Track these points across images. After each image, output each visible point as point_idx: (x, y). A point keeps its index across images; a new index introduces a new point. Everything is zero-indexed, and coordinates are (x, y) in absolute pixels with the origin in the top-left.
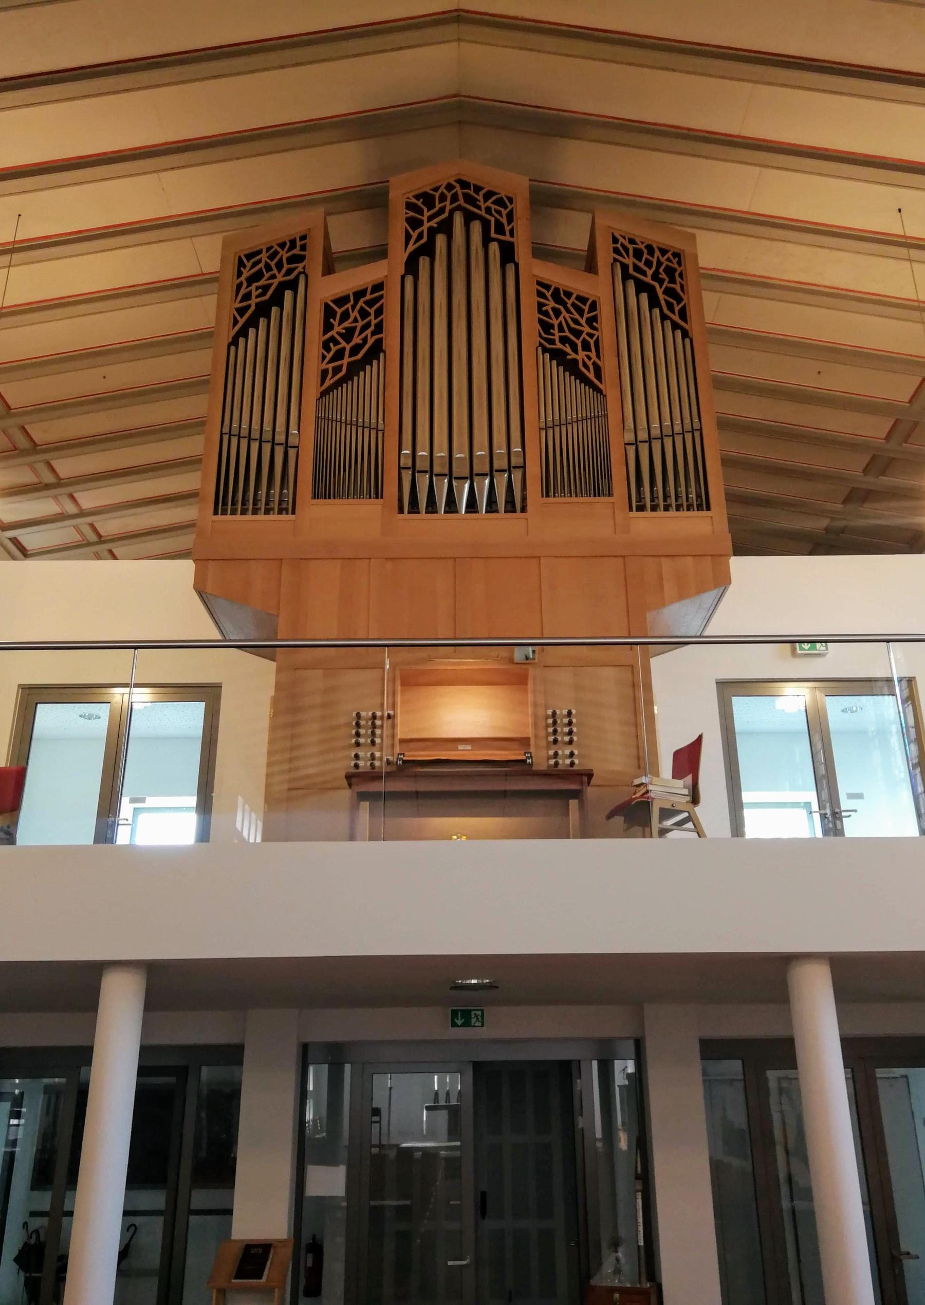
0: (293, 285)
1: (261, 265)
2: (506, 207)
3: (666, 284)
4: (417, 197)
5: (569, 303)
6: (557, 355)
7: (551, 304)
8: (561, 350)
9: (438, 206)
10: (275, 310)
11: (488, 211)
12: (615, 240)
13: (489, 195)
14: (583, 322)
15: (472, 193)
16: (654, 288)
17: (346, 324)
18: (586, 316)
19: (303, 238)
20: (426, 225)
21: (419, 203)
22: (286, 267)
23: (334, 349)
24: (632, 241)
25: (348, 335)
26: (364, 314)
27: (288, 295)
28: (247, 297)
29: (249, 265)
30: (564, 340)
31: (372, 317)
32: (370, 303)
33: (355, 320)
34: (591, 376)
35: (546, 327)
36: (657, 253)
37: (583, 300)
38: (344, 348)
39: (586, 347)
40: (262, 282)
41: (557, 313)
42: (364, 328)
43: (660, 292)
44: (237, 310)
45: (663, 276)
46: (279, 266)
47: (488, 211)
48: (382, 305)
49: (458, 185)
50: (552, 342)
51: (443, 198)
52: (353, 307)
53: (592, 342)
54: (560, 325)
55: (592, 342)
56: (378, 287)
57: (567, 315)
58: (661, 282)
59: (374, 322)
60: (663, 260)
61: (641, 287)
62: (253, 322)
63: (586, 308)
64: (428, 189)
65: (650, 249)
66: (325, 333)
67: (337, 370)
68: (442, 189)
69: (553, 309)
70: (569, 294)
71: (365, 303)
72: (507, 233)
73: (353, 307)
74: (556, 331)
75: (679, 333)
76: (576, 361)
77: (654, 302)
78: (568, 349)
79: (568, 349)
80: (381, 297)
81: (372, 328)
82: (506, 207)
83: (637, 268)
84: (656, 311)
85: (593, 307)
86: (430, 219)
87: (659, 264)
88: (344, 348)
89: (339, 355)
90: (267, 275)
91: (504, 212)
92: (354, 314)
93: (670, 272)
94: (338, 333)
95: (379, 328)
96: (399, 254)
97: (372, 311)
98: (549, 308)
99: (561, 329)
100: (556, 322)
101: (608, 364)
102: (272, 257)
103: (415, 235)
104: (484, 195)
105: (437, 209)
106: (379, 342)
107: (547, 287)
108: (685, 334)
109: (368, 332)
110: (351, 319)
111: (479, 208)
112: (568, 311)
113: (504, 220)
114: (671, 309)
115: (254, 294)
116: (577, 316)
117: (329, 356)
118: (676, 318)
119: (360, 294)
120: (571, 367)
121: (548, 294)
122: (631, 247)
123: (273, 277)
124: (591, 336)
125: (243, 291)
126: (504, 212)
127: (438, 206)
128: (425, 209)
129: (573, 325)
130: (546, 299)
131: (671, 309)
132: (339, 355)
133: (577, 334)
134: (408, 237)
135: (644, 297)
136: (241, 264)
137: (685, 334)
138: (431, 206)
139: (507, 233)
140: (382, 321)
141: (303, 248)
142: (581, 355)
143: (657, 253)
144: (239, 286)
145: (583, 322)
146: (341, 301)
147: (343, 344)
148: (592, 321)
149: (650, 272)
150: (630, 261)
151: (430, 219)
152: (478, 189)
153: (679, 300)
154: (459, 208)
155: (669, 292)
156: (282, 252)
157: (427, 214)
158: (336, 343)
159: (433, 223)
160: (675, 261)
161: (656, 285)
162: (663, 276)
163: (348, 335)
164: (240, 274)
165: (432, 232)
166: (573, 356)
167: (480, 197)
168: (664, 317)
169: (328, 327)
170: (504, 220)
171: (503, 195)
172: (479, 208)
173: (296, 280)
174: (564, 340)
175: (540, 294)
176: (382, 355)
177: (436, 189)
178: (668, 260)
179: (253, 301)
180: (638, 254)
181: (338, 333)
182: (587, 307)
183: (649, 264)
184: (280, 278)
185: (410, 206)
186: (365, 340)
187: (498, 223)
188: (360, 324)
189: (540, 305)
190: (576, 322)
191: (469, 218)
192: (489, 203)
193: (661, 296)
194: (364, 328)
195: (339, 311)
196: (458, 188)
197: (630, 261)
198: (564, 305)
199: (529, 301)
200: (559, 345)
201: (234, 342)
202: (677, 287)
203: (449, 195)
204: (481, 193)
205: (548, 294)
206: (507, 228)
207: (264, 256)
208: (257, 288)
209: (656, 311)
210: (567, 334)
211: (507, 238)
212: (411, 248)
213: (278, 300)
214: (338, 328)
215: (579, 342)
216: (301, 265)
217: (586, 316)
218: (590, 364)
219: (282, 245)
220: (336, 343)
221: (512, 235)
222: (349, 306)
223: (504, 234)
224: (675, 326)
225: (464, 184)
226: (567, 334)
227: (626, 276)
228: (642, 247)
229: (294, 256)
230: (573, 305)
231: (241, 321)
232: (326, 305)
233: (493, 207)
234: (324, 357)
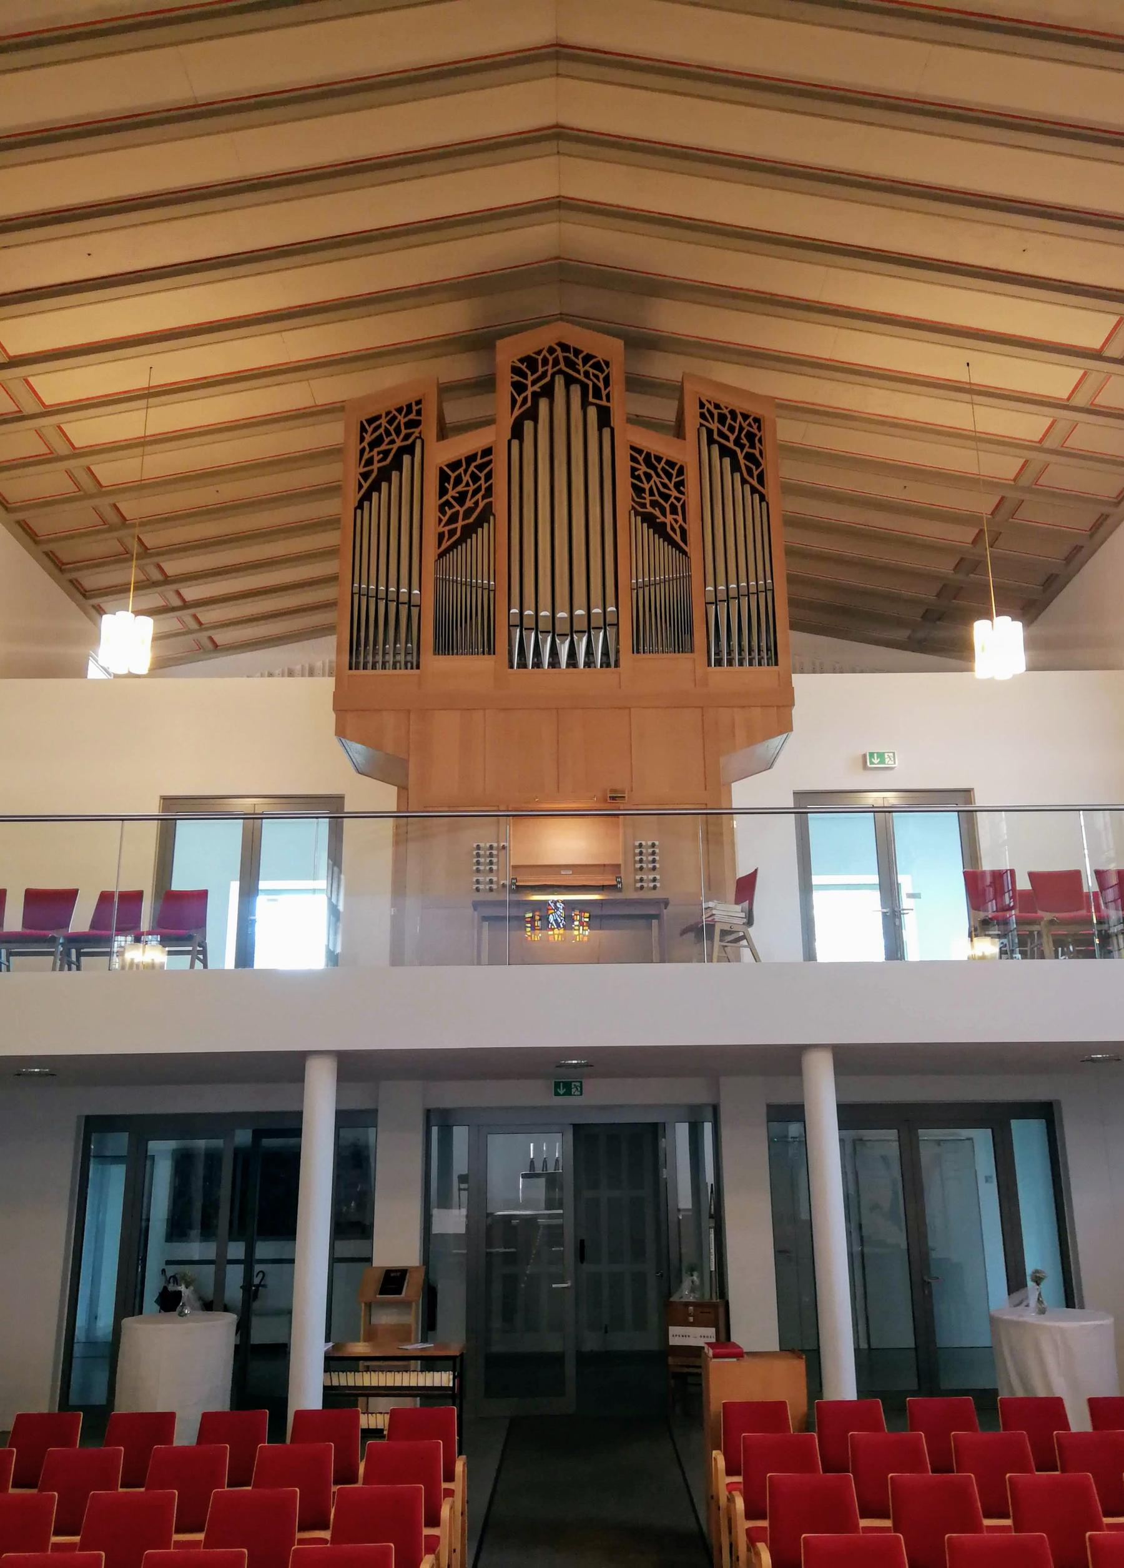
1: (382, 430)
2: (602, 371)
5: (660, 467)
7: (643, 468)
8: (651, 513)
12: (702, 406)
13: (588, 358)
14: (671, 486)
15: (571, 356)
16: (735, 452)
17: (460, 488)
18: (674, 480)
19: (418, 403)
20: (530, 390)
21: (523, 367)
23: (449, 512)
25: (461, 499)
26: (475, 478)
28: (370, 462)
29: (370, 430)
31: (482, 481)
32: (481, 468)
33: (467, 485)
35: (638, 490)
36: (740, 418)
38: (458, 512)
39: (674, 511)
40: (383, 447)
41: (649, 477)
42: (476, 492)
43: (741, 457)
45: (744, 441)
48: (491, 470)
49: (558, 349)
50: (644, 506)
52: (466, 471)
53: (679, 505)
54: (651, 489)
55: (679, 505)
56: (488, 452)
57: (657, 480)
58: (742, 447)
60: (744, 425)
61: (725, 452)
63: (674, 473)
67: (452, 533)
68: (545, 352)
69: (645, 473)
70: (659, 459)
71: (476, 467)
72: (604, 398)
73: (466, 471)
74: (647, 495)
77: (735, 467)
78: (657, 513)
79: (657, 513)
80: (490, 462)
82: (602, 371)
83: (721, 434)
87: (741, 429)
88: (458, 512)
89: (453, 519)
91: (601, 376)
92: (466, 478)
93: (751, 437)
94: (452, 497)
98: (640, 472)
99: (652, 494)
100: (647, 486)
103: (520, 399)
104: (583, 358)
105: (540, 373)
106: (490, 504)
107: (640, 451)
108: (762, 498)
109: (479, 496)
110: (464, 483)
111: (578, 372)
112: (658, 476)
113: (601, 385)
114: (751, 476)
115: (376, 459)
116: (666, 481)
117: (445, 519)
118: (755, 483)
119: (471, 459)
121: (641, 459)
124: (678, 499)
125: (366, 456)
126: (601, 376)
127: (541, 370)
128: (529, 373)
129: (662, 489)
130: (638, 462)
132: (453, 519)
133: (666, 497)
134: (514, 401)
136: (363, 429)
137: (762, 498)
138: (534, 370)
139: (604, 398)
140: (491, 485)
141: (419, 413)
143: (740, 418)
144: (362, 451)
145: (671, 486)
147: (457, 507)
148: (679, 485)
149: (732, 437)
150: (715, 426)
152: (577, 352)
154: (560, 372)
155: (749, 457)
160: (755, 426)
161: (738, 450)
162: (744, 441)
163: (461, 499)
164: (362, 439)
166: (662, 519)
167: (580, 362)
168: (744, 482)
169: (443, 491)
170: (601, 385)
172: (578, 372)
174: (654, 504)
176: (492, 518)
177: (539, 353)
178: (750, 425)
181: (452, 497)
184: (399, 443)
185: (515, 370)
186: (477, 503)
187: (595, 386)
188: (472, 487)
189: (633, 469)
190: (665, 486)
191: (569, 381)
192: (587, 367)
193: (742, 462)
194: (476, 492)
195: (453, 475)
197: (715, 426)
198: (655, 469)
199: (624, 464)
200: (650, 509)
203: (551, 359)
204: (580, 357)
205: (641, 459)
206: (604, 393)
208: (379, 453)
211: (604, 403)
212: (517, 413)
214: (452, 493)
215: (667, 506)
216: (417, 431)
218: (676, 526)
220: (451, 507)
221: (608, 400)
222: (461, 470)
223: (601, 399)
224: (754, 490)
225: (565, 347)
226: (657, 497)
228: (726, 411)
229: (411, 421)
230: (663, 469)
231: (366, 485)
232: (441, 469)
234: (440, 520)
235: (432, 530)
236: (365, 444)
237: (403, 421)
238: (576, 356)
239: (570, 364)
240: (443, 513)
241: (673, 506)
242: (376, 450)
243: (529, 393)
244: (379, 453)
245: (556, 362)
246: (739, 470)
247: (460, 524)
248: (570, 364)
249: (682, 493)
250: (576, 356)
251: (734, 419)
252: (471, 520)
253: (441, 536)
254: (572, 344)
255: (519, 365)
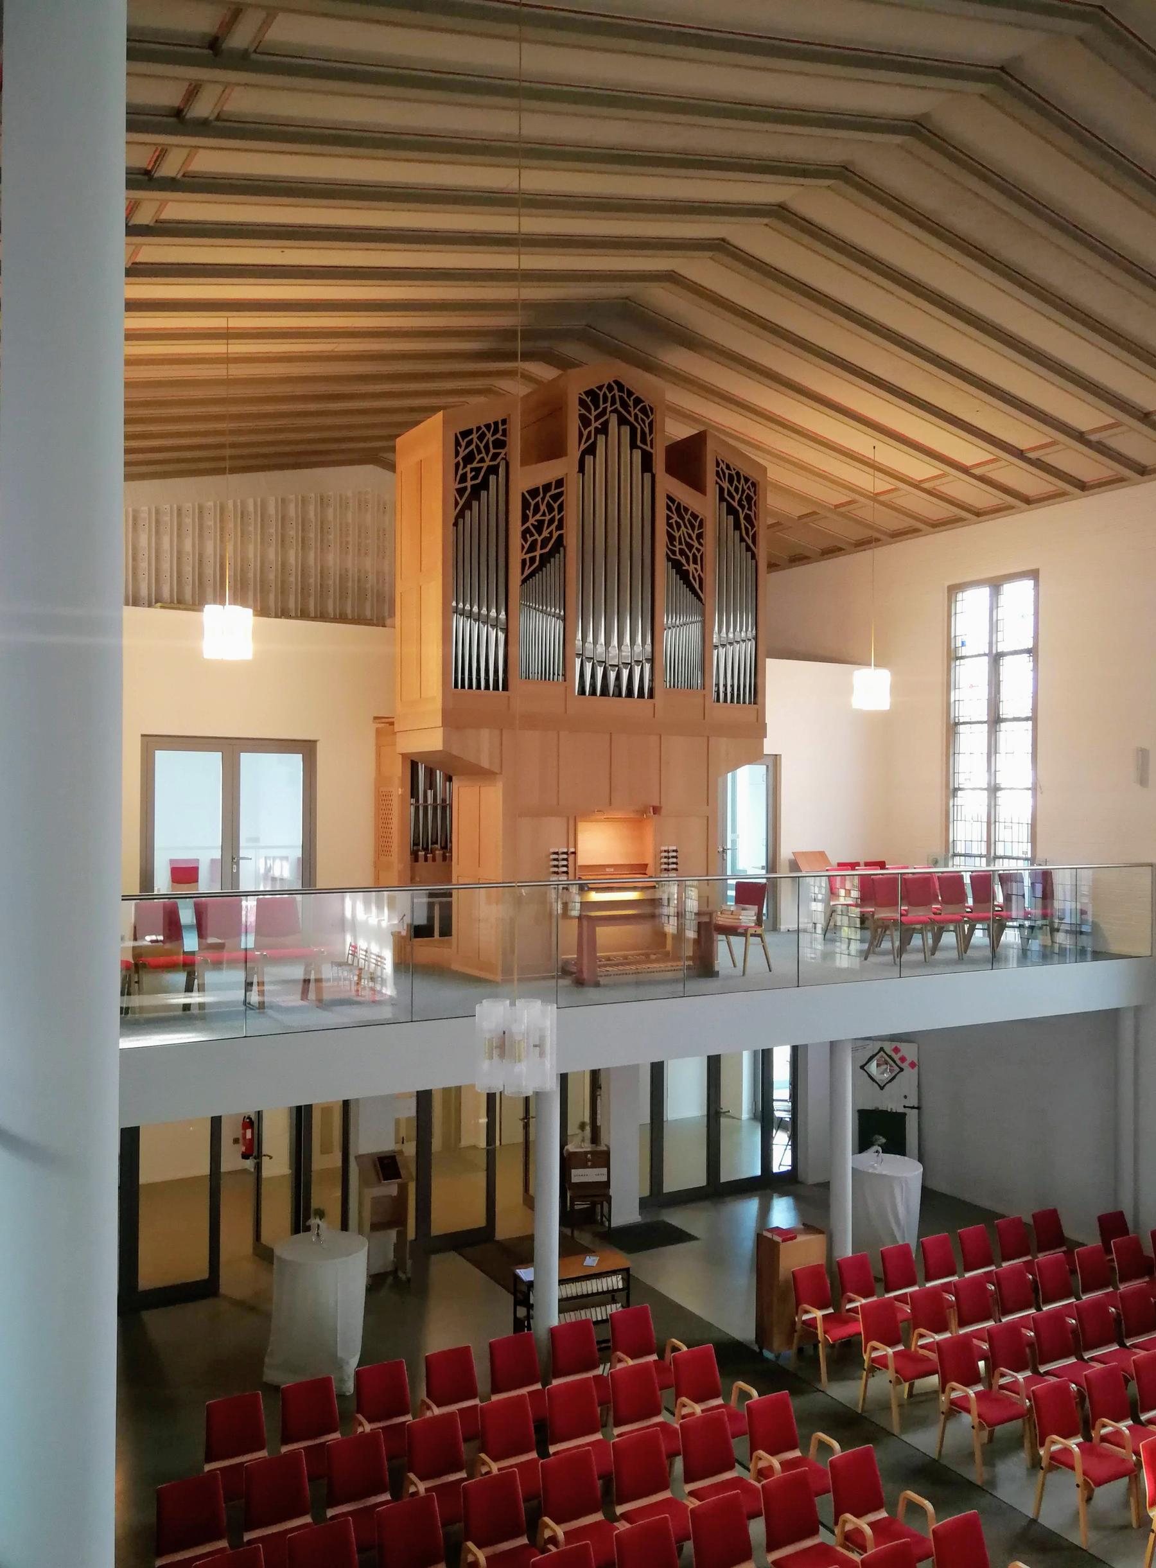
0: (493, 470)
1: (473, 446)
2: (648, 417)
3: (746, 511)
4: (587, 393)
5: (686, 518)
6: (676, 565)
7: (675, 517)
9: (602, 406)
10: (484, 494)
11: (636, 415)
12: (718, 465)
13: (638, 401)
14: (694, 537)
17: (538, 517)
18: (696, 532)
19: (504, 422)
22: (492, 451)
23: (530, 540)
24: (728, 467)
25: (539, 527)
26: (550, 508)
27: (492, 478)
28: (463, 479)
29: (464, 444)
30: (682, 552)
31: (556, 512)
32: (555, 497)
33: (544, 514)
34: (697, 586)
35: (671, 538)
36: (742, 481)
37: (695, 516)
39: (695, 562)
40: (475, 465)
42: (551, 521)
43: (742, 517)
44: (457, 490)
46: (487, 447)
47: (636, 415)
50: (674, 552)
51: (605, 395)
52: (543, 499)
53: (699, 556)
55: (699, 556)
56: (560, 483)
58: (743, 507)
59: (557, 517)
61: (731, 510)
62: (468, 506)
63: (697, 525)
64: (594, 387)
65: (738, 474)
66: (523, 524)
67: (532, 560)
68: (604, 389)
70: (686, 510)
73: (543, 499)
74: (677, 544)
75: (749, 554)
76: (687, 571)
77: (737, 526)
78: (684, 562)
79: (684, 562)
80: (561, 494)
81: (556, 523)
82: (648, 417)
84: (737, 533)
85: (701, 526)
86: (597, 418)
87: (743, 491)
89: (532, 548)
90: (478, 458)
91: (647, 422)
92: (543, 508)
93: (749, 498)
95: (560, 527)
96: (574, 449)
97: (556, 506)
98: (672, 521)
99: (680, 543)
100: (677, 535)
101: (710, 579)
102: (481, 437)
103: (585, 433)
106: (561, 536)
108: (753, 556)
109: (553, 526)
113: (647, 430)
114: (747, 534)
115: (469, 476)
117: (527, 546)
118: (750, 542)
119: (547, 488)
120: (684, 576)
121: (674, 508)
122: (727, 472)
123: (482, 460)
124: (698, 550)
125: (460, 472)
126: (647, 422)
127: (602, 406)
131: (747, 534)
132: (532, 548)
133: (690, 547)
134: (581, 435)
135: (731, 518)
136: (458, 444)
141: (504, 433)
142: (691, 568)
143: (742, 481)
144: (457, 465)
145: (694, 537)
146: (534, 493)
147: (536, 536)
148: (700, 536)
149: (737, 497)
150: (726, 485)
151: (597, 418)
152: (630, 394)
153: (753, 526)
154: (615, 411)
155: (748, 518)
156: (489, 435)
157: (594, 413)
158: (532, 535)
159: (597, 424)
163: (539, 527)
165: (598, 431)
167: (631, 403)
168: (742, 540)
169: (525, 518)
170: (647, 430)
171: (646, 403)
173: (498, 466)
174: (682, 552)
175: (669, 508)
177: (600, 388)
179: (469, 484)
180: (731, 481)
182: (697, 522)
183: (737, 489)
184: (488, 463)
185: (582, 403)
186: (551, 533)
187: (643, 432)
188: (547, 518)
189: (669, 518)
190: (690, 537)
191: (622, 421)
193: (743, 521)
195: (533, 503)
196: (616, 391)
197: (726, 485)
198: (683, 519)
200: (679, 557)
201: (456, 524)
202: (752, 514)
203: (609, 396)
205: (674, 508)
206: (649, 439)
207: (474, 436)
208: (472, 470)
209: (737, 533)
210: (684, 547)
211: (648, 448)
212: (583, 447)
213: (485, 485)
214: (532, 521)
215: (690, 555)
216: (503, 451)
217: (696, 532)
219: (488, 426)
220: (532, 535)
222: (539, 499)
224: (748, 549)
225: (621, 387)
226: (684, 547)
227: (722, 499)
228: (733, 473)
231: (461, 503)
233: (640, 415)
234: (523, 547)
235: (517, 556)
236: (459, 458)
237: (491, 439)
238: (629, 397)
239: (624, 405)
240: (526, 541)
241: (694, 556)
242: (469, 466)
243: (592, 428)
244: (472, 470)
245: (613, 403)
246: (740, 529)
247: (537, 553)
248: (624, 405)
249: (701, 544)
250: (629, 397)
251: (739, 481)
252: (547, 550)
253: (524, 562)
254: (627, 385)
255: (584, 397)
